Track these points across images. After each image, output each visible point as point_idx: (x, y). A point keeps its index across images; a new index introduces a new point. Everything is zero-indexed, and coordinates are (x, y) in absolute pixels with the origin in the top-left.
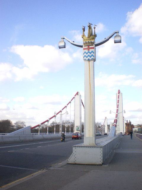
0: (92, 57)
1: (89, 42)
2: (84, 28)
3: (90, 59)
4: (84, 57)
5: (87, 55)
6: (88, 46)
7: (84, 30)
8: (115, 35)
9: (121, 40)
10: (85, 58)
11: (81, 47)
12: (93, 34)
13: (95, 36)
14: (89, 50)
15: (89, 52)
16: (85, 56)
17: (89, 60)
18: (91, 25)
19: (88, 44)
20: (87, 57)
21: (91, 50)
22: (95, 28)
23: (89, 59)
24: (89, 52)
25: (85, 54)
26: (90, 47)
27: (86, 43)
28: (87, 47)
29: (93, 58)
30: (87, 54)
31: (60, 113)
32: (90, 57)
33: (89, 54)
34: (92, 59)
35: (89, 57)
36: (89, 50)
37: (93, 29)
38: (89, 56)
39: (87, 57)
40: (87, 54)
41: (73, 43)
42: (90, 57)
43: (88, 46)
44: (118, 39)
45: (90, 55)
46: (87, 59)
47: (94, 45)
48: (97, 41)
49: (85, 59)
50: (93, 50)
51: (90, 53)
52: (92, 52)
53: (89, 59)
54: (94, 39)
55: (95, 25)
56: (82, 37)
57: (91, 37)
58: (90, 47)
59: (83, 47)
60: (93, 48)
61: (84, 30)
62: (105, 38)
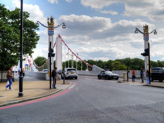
3: (52, 34)
5: (50, 33)
6: (51, 28)
7: (48, 19)
14: (51, 30)
16: (50, 33)
19: (51, 28)
21: (52, 30)
24: (51, 31)
33: (51, 32)
35: (51, 34)
36: (51, 30)
38: (51, 33)
39: (50, 34)
40: (50, 32)
43: (51, 28)
45: (52, 33)
46: (50, 34)
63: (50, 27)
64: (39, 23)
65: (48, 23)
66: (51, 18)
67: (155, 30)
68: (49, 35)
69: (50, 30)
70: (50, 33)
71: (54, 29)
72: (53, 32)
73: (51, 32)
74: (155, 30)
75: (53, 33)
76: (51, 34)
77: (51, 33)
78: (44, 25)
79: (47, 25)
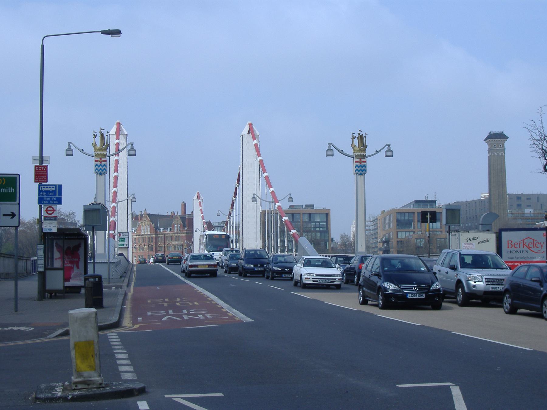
3: (102, 173)
5: (99, 169)
14: (101, 163)
16: (97, 169)
20: (99, 171)
21: (103, 163)
24: (101, 165)
26: (102, 159)
28: (99, 159)
30: (99, 166)
32: (102, 171)
33: (101, 167)
35: (101, 171)
36: (101, 163)
37: (106, 137)
38: (101, 169)
40: (99, 166)
42: (102, 171)
43: (101, 158)
45: (103, 169)
46: (99, 172)
51: (103, 167)
52: (104, 165)
61: (95, 136)
63: (98, 155)
65: (94, 145)
66: (101, 132)
67: (389, 145)
69: (98, 163)
70: (99, 169)
73: (101, 167)
74: (389, 145)
75: (104, 169)
77: (101, 169)
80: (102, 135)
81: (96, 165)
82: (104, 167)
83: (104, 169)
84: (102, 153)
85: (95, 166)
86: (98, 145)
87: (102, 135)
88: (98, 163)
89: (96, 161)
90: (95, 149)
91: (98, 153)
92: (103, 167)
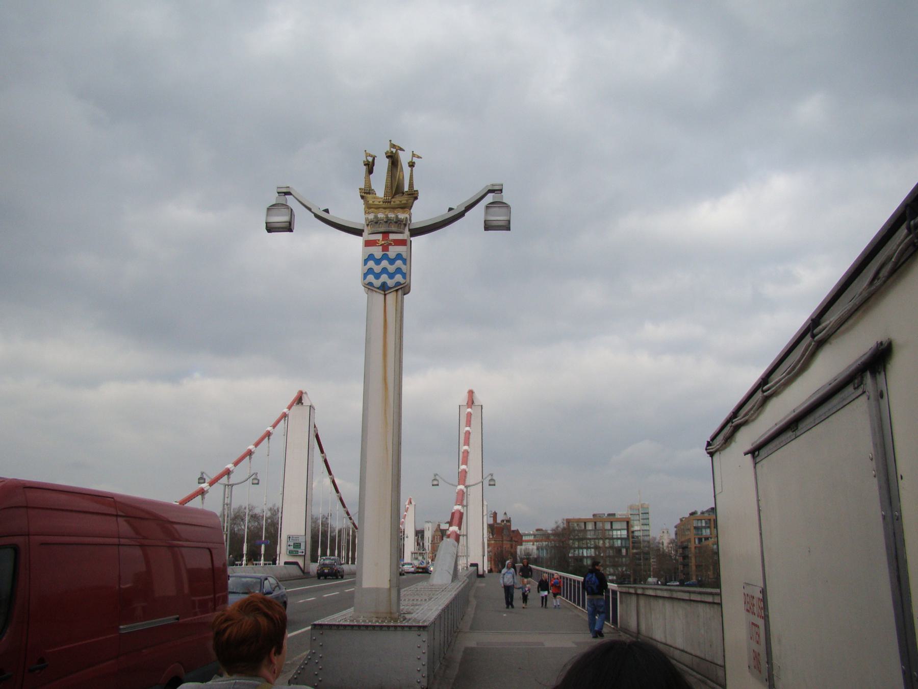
0: (399, 278)
1: (388, 221)
2: (370, 159)
3: (390, 283)
4: (365, 276)
6: (386, 234)
7: (370, 167)
8: (490, 198)
9: (509, 221)
10: (371, 278)
11: (358, 232)
12: (406, 189)
13: (414, 195)
14: (385, 248)
15: (385, 257)
16: (370, 271)
17: (384, 288)
18: (400, 153)
20: (377, 276)
21: (393, 251)
22: (412, 165)
23: (384, 284)
24: (385, 257)
25: (371, 264)
27: (376, 222)
29: (402, 281)
30: (378, 262)
31: (224, 480)
32: (391, 276)
33: (385, 263)
34: (398, 284)
35: (384, 278)
36: (385, 248)
37: (406, 170)
38: (384, 270)
39: (377, 276)
40: (378, 262)
41: (325, 215)
42: (391, 276)
43: (386, 234)
44: (498, 217)
45: (391, 269)
46: (377, 283)
47: (407, 233)
48: (420, 214)
49: (370, 284)
50: (401, 249)
51: (392, 262)
52: (399, 256)
53: (384, 284)
54: (407, 207)
55: (414, 155)
56: (362, 197)
57: (398, 200)
58: (392, 237)
59: (365, 234)
60: (403, 243)
61: (370, 167)
62: (450, 209)
64: (290, 201)
65: (366, 192)
68: (369, 286)
69: (377, 252)
70: (377, 269)
71: (417, 241)
72: (405, 261)
73: (385, 263)
75: (399, 270)
76: (384, 278)
78: (335, 215)
79: (356, 214)
80: (394, 160)
81: (371, 257)
82: (399, 263)
83: (399, 270)
84: (392, 215)
85: (366, 262)
86: (380, 191)
87: (394, 160)
88: (377, 252)
89: (368, 244)
90: (369, 207)
91: (376, 217)
92: (392, 262)
